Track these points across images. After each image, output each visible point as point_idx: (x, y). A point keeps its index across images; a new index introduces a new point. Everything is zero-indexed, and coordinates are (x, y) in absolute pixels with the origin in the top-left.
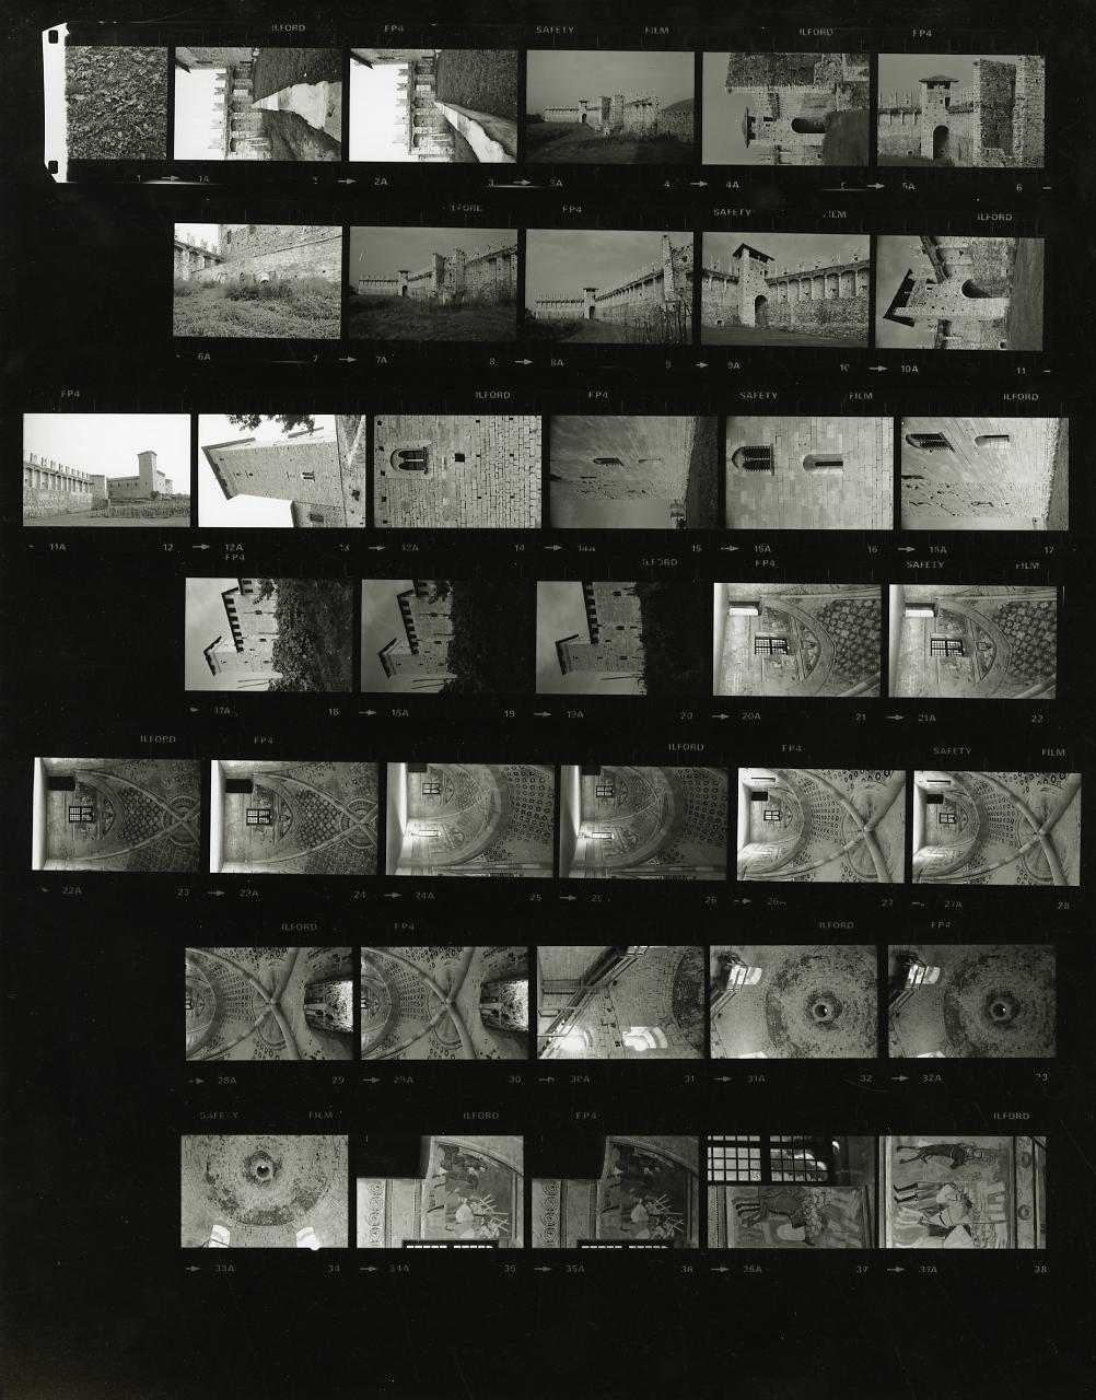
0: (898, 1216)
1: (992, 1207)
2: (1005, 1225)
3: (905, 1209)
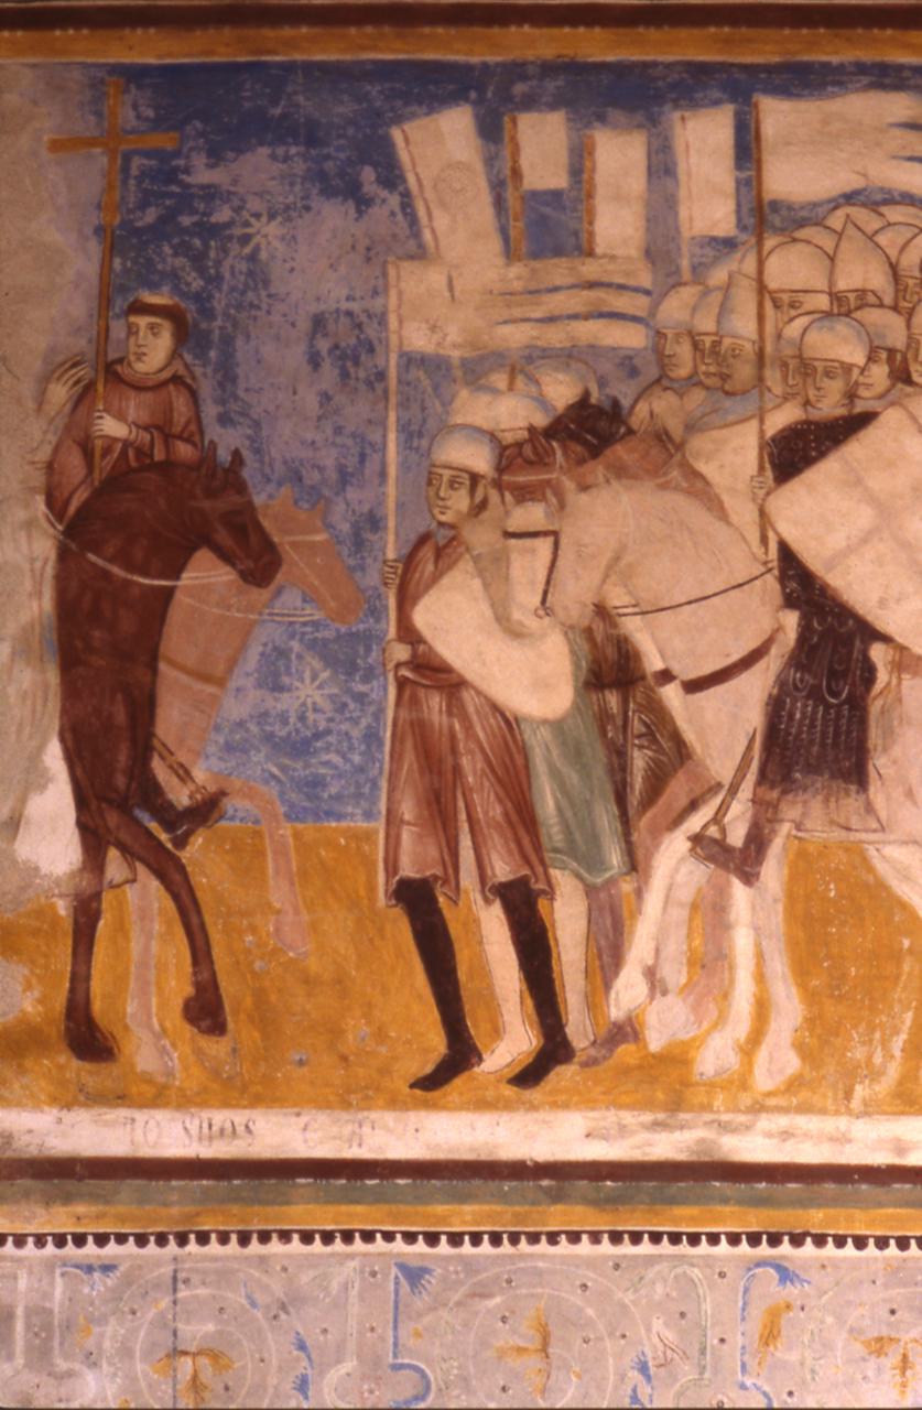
0: (677, 1059)
1: (617, 225)
2: (777, 115)
3: (628, 991)
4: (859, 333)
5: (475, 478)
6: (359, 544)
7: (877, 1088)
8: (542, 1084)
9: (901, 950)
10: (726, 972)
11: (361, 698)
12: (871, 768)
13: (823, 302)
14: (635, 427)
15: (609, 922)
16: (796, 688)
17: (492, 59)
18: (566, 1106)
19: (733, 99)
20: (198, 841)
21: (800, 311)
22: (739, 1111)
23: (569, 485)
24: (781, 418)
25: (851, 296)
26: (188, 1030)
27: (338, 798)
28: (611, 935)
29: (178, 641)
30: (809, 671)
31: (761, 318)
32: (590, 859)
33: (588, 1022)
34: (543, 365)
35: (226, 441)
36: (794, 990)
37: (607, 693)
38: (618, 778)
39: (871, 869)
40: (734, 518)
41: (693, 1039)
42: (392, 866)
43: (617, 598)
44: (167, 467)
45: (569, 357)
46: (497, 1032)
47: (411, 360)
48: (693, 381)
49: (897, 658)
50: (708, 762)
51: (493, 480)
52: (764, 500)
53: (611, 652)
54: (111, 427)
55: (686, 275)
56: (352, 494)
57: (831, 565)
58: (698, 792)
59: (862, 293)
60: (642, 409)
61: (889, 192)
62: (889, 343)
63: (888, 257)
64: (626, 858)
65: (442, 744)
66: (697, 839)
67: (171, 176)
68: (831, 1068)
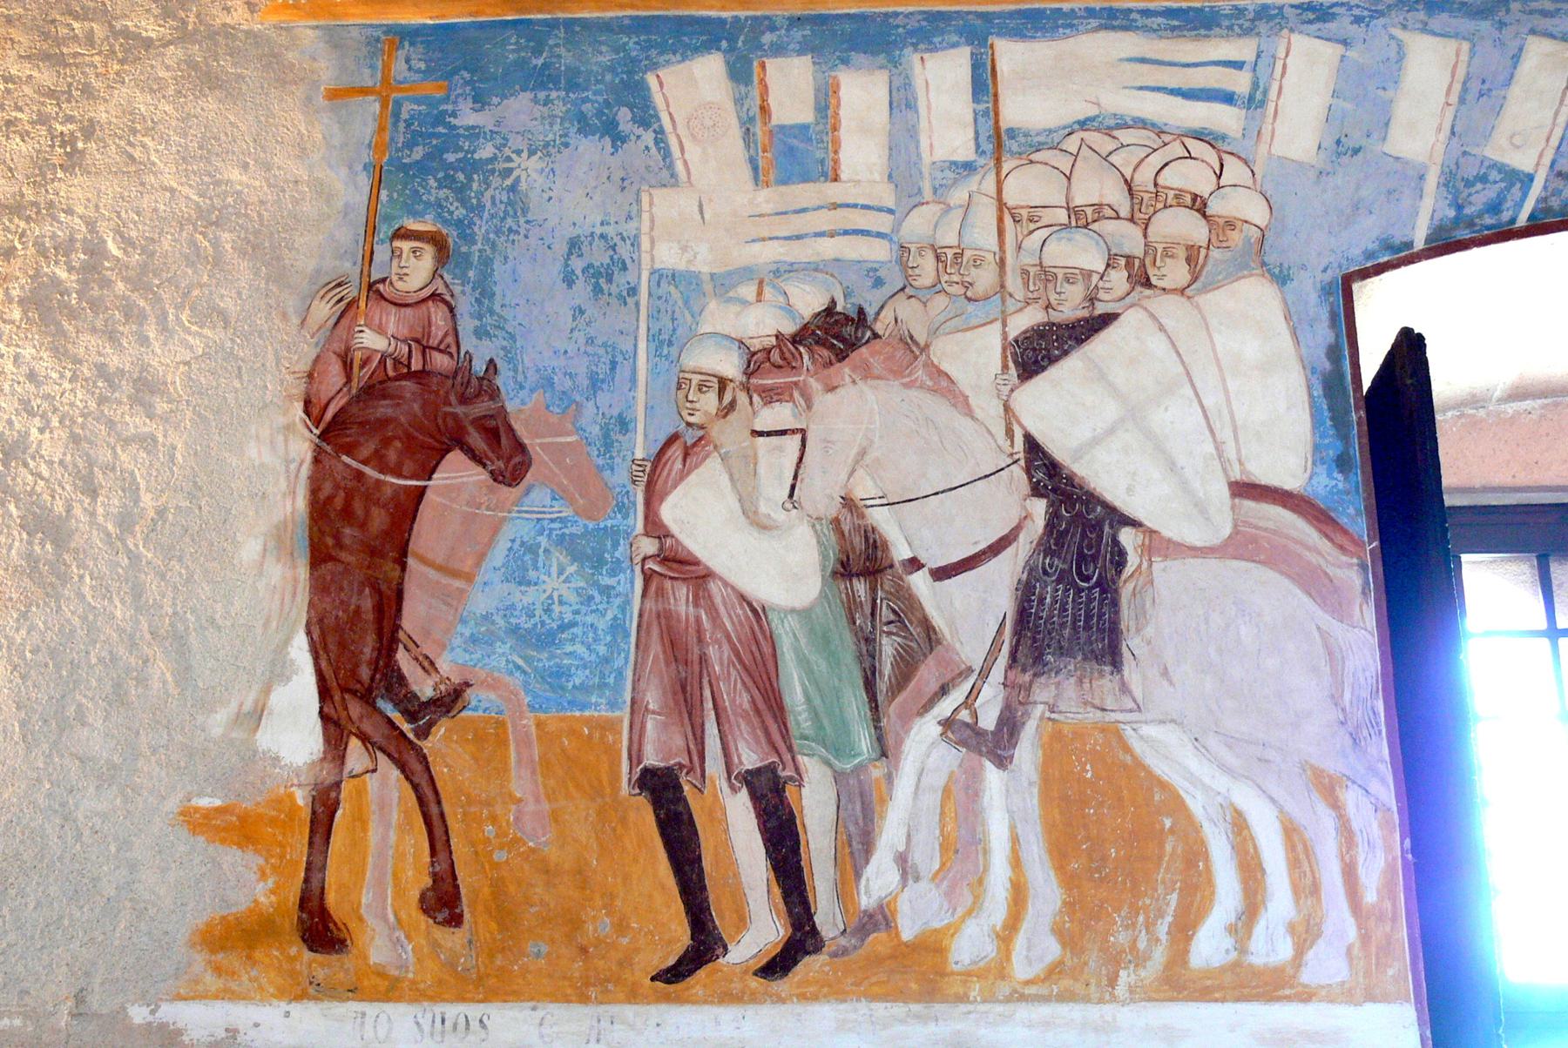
0: (932, 948)
1: (862, 156)
2: (1010, 54)
3: (879, 879)
5: (723, 383)
6: (608, 444)
7: (1143, 974)
10: (981, 857)
11: (606, 591)
12: (1124, 649)
13: (1062, 216)
15: (858, 807)
16: (1045, 572)
17: (742, 14)
18: (815, 998)
19: (969, 43)
20: (440, 731)
23: (815, 385)
24: (1024, 320)
25: (1089, 211)
26: (423, 921)
27: (584, 688)
29: (427, 535)
31: (1001, 232)
32: (838, 746)
35: (480, 352)
36: (1052, 873)
37: (855, 581)
38: (867, 665)
39: (1127, 749)
40: (979, 413)
41: (948, 927)
42: (635, 756)
43: (864, 488)
44: (422, 376)
45: (815, 268)
46: (742, 922)
47: (659, 276)
48: (936, 288)
50: (958, 646)
51: (741, 383)
53: (859, 543)
54: (371, 340)
55: (928, 194)
56: (603, 398)
57: (1078, 454)
58: (949, 677)
60: (887, 315)
62: (1127, 251)
64: (876, 745)
65: (691, 636)
66: (947, 723)
67: (440, 119)
68: (1093, 958)
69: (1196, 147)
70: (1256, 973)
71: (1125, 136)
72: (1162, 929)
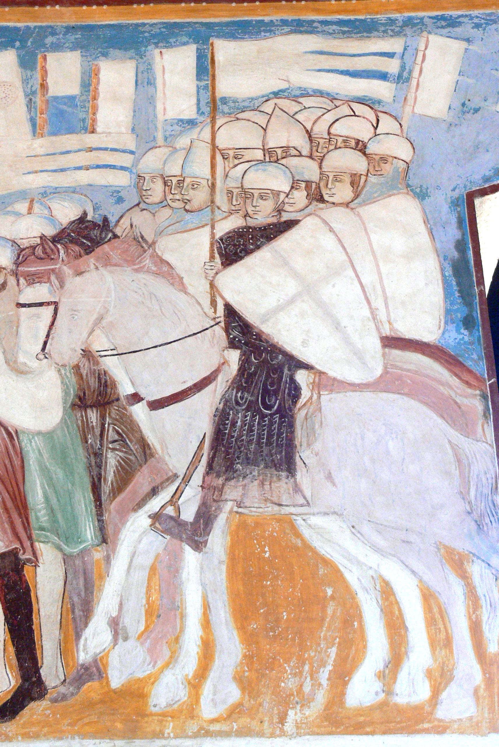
0: (136, 693)
1: (113, 116)
2: (224, 50)
3: (96, 638)
4: (285, 173)
7: (307, 712)
8: (18, 718)
9: (326, 596)
10: (178, 620)
12: (297, 459)
13: (259, 155)
14: (119, 234)
15: (82, 582)
16: (237, 403)
17: (32, 24)
18: (36, 736)
19: (196, 42)
21: (241, 160)
22: (187, 737)
23: (67, 270)
24: (226, 226)
25: (279, 151)
28: (83, 594)
30: (248, 392)
31: (213, 166)
32: (69, 535)
33: (60, 664)
34: (54, 197)
36: (235, 633)
37: (89, 411)
38: (95, 473)
39: (298, 535)
40: (190, 290)
41: (149, 677)
43: (100, 343)
45: (74, 190)
48: (163, 203)
49: (317, 379)
50: (167, 458)
51: (12, 271)
52: (214, 277)
53: (93, 383)
55: (160, 141)
57: (265, 319)
58: (159, 481)
59: (286, 149)
60: (125, 223)
61: (305, 90)
62: (307, 178)
63: (305, 128)
64: (98, 534)
66: (156, 517)
68: (267, 700)
69: (359, 108)
70: (400, 710)
71: (307, 102)
72: (324, 675)
